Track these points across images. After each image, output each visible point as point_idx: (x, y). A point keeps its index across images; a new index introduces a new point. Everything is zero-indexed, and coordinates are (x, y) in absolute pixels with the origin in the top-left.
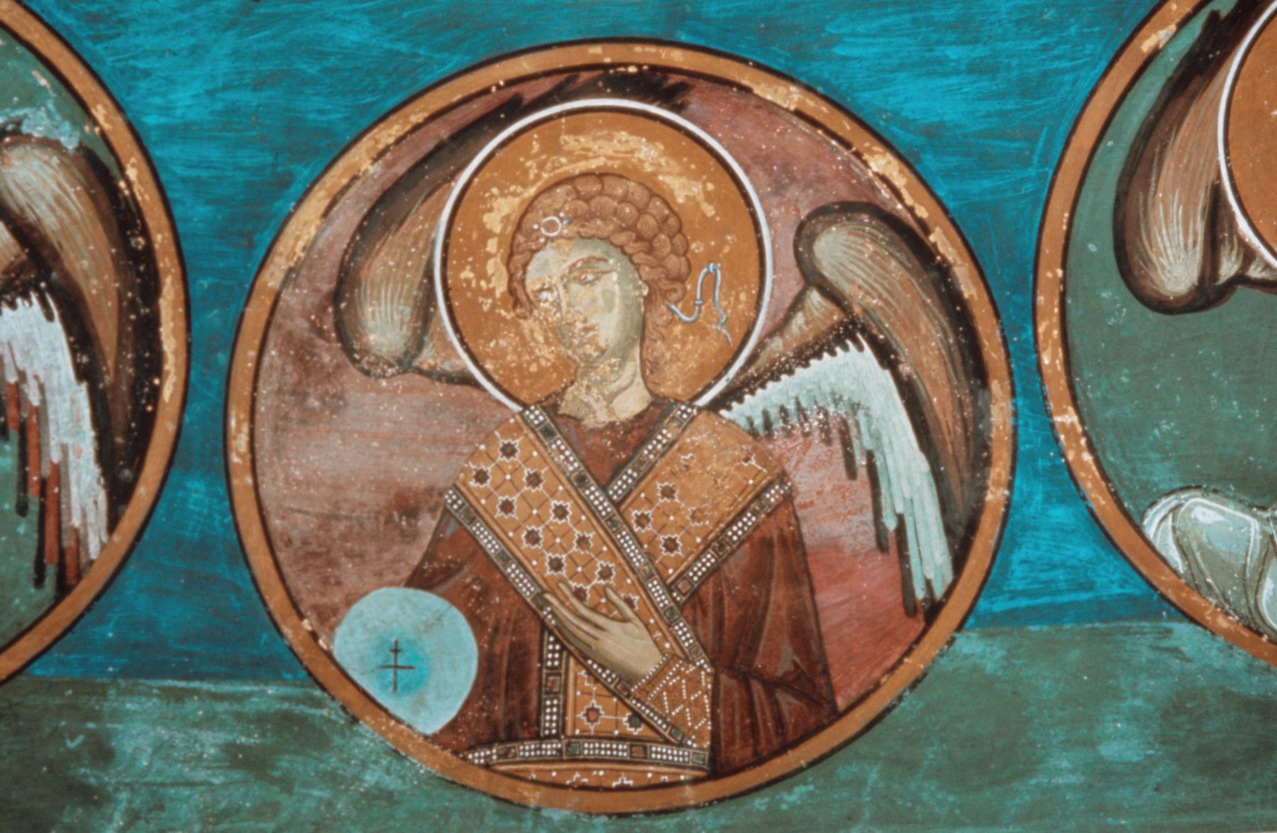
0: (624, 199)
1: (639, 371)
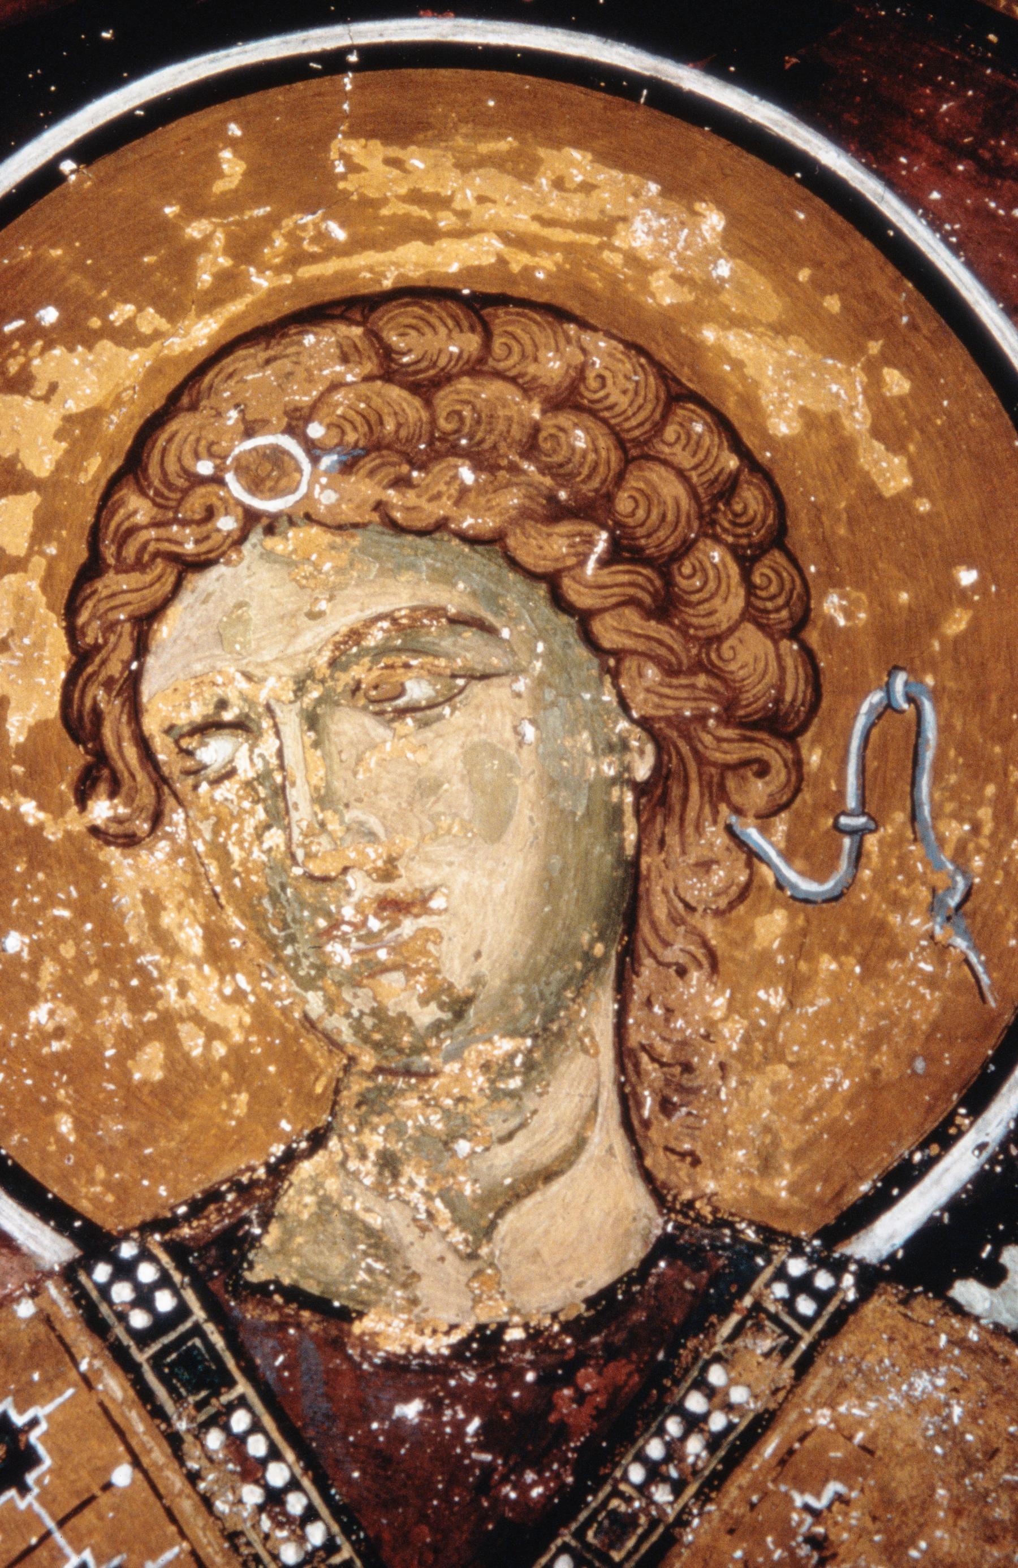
0: (569, 398)
1: (609, 1097)
